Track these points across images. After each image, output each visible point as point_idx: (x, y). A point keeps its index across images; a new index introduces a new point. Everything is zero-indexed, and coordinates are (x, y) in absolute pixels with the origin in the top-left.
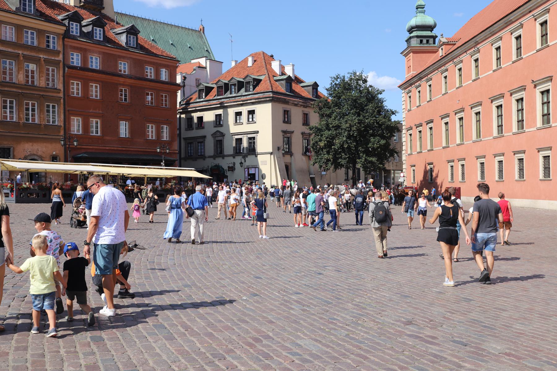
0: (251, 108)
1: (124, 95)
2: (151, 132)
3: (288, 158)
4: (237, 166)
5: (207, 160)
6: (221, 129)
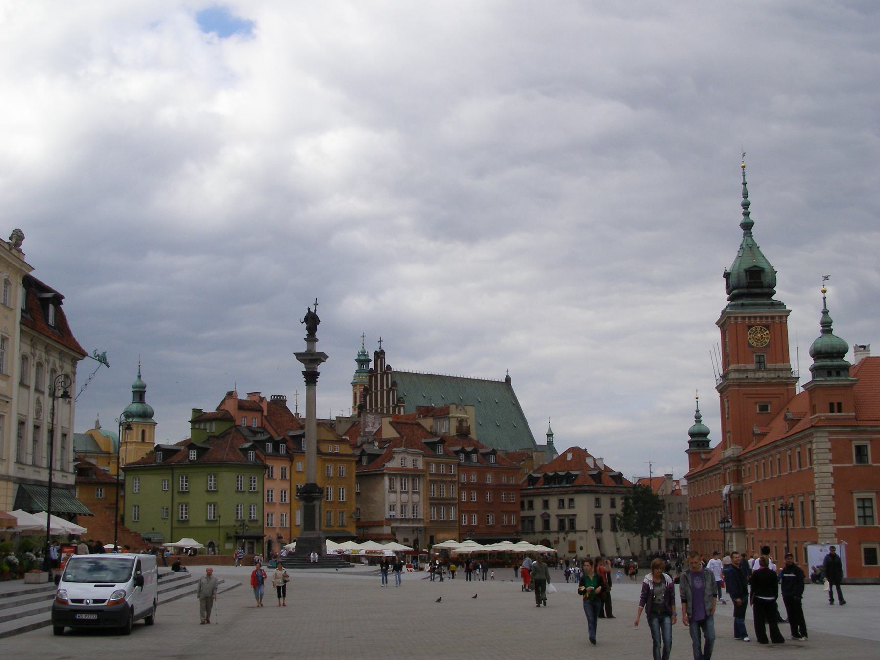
0: (572, 496)
1: (489, 497)
2: (505, 519)
3: (599, 534)
4: (561, 540)
5: (537, 535)
6: (547, 511)
